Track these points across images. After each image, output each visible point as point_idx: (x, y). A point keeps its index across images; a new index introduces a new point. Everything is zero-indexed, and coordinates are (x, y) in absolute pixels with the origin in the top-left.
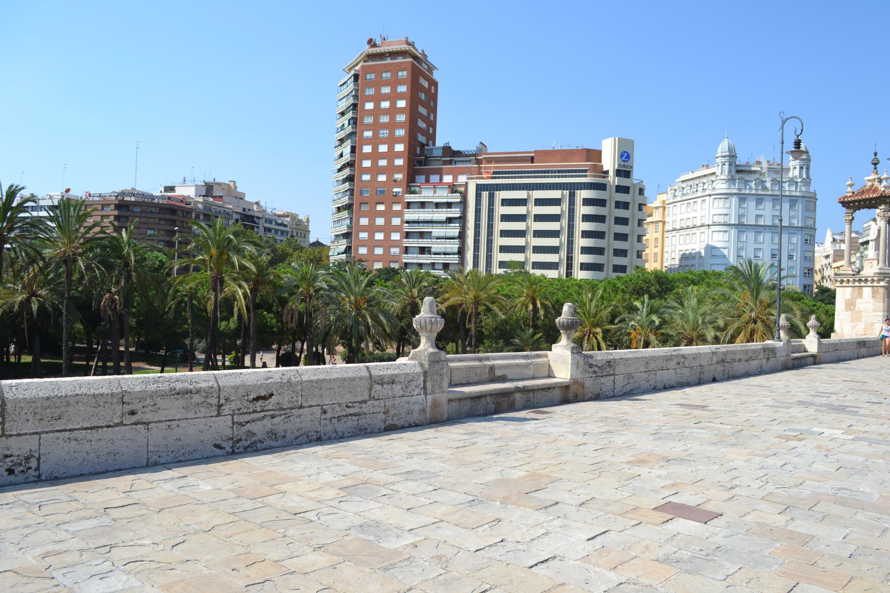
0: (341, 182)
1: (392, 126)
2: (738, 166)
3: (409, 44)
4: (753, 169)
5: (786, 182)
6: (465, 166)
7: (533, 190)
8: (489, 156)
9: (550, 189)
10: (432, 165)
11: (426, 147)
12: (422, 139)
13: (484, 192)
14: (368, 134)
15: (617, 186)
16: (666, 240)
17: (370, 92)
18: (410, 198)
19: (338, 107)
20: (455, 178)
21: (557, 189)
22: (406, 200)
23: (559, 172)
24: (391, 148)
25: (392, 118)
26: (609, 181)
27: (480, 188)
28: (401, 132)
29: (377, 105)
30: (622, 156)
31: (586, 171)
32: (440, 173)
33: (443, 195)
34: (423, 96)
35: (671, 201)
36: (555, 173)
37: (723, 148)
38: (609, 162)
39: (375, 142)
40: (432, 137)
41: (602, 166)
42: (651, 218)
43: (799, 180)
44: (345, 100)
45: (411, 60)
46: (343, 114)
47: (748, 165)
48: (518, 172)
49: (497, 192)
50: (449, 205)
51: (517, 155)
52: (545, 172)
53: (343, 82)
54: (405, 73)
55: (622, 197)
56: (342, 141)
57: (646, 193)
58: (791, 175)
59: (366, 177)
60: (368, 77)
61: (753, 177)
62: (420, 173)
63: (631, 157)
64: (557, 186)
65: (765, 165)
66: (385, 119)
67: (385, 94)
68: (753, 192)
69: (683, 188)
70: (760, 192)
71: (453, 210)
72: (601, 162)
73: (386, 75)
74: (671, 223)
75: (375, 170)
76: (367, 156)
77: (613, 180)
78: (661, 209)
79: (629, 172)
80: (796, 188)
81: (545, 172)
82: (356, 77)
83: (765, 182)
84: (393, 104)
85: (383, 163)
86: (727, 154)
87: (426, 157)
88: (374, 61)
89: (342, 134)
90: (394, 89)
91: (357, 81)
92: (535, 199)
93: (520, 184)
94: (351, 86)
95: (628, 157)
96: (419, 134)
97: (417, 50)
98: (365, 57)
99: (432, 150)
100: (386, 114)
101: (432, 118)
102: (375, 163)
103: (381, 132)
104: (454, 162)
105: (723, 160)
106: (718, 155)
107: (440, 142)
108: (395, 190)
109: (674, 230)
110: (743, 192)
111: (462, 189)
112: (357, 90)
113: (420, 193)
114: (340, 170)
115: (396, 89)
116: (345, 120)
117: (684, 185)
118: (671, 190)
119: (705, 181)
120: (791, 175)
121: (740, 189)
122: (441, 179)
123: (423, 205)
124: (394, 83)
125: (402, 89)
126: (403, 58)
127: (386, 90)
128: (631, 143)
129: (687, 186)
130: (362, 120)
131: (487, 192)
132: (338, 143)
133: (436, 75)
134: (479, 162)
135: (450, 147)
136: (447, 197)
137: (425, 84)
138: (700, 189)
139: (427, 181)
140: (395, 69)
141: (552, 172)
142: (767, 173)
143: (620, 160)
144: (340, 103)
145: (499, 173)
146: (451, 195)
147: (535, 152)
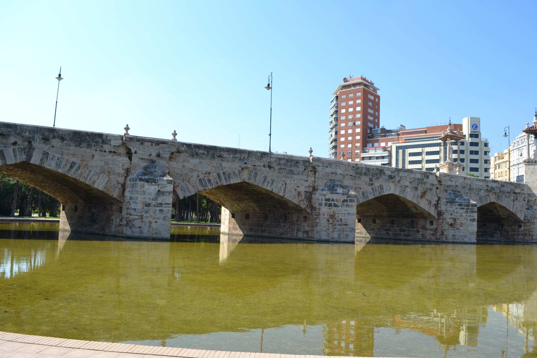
0: (331, 149)
3: (362, 78)
6: (391, 137)
7: (425, 147)
8: (407, 131)
9: (434, 146)
10: (376, 138)
11: (373, 129)
12: (371, 125)
13: (400, 150)
14: (343, 125)
15: (470, 143)
16: (511, 172)
17: (343, 104)
18: (363, 155)
20: (387, 144)
21: (437, 146)
22: (362, 156)
26: (466, 140)
27: (398, 148)
28: (358, 123)
29: (347, 110)
30: (473, 126)
33: (380, 153)
34: (371, 104)
35: (512, 149)
36: (437, 138)
38: (466, 131)
39: (346, 128)
40: (378, 124)
41: (463, 133)
42: (503, 159)
44: (332, 109)
45: (362, 87)
46: (332, 115)
48: (418, 139)
49: (407, 150)
50: (383, 157)
51: (418, 130)
52: (432, 138)
53: (332, 100)
54: (360, 94)
55: (474, 148)
56: (332, 129)
57: (490, 146)
59: (342, 146)
60: (343, 97)
62: (369, 142)
63: (478, 127)
64: (434, 145)
67: (351, 105)
69: (518, 142)
71: (384, 160)
72: (462, 131)
73: (351, 95)
74: (512, 161)
75: (346, 142)
76: (343, 136)
77: (468, 139)
78: (508, 154)
79: (478, 135)
81: (432, 138)
82: (337, 97)
84: (355, 109)
87: (372, 134)
88: (345, 89)
89: (332, 126)
90: (355, 102)
91: (338, 99)
92: (426, 152)
93: (415, 145)
94: (335, 102)
95: (476, 127)
96: (369, 123)
97: (368, 82)
98: (341, 87)
99: (378, 130)
100: (352, 114)
101: (377, 114)
102: (346, 139)
103: (349, 123)
107: (380, 127)
108: (356, 151)
109: (514, 165)
111: (389, 149)
112: (337, 104)
113: (369, 152)
114: (332, 143)
115: (356, 102)
116: (332, 119)
122: (380, 145)
123: (370, 158)
124: (355, 99)
125: (359, 101)
126: (360, 86)
127: (351, 103)
128: (479, 119)
129: (520, 140)
130: (340, 118)
131: (402, 150)
132: (330, 130)
133: (379, 93)
134: (398, 135)
135: (384, 129)
136: (381, 153)
137: (372, 98)
139: (373, 146)
140: (355, 92)
143: (472, 129)
144: (331, 110)
145: (407, 140)
146: (383, 152)
147: (427, 128)
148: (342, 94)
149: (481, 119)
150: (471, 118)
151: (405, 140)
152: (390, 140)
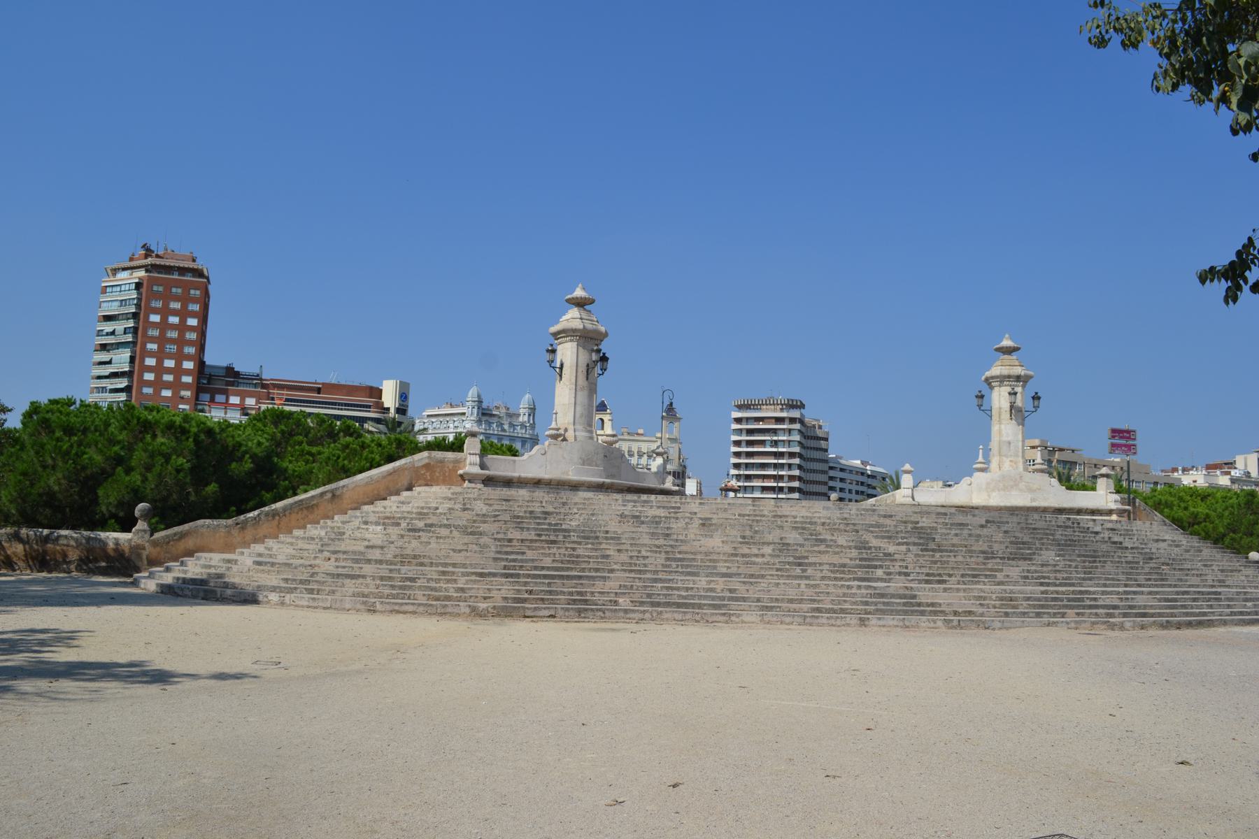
1: (181, 342)
2: (483, 409)
4: (494, 413)
5: (518, 426)
17: (158, 304)
19: (100, 307)
20: (243, 400)
23: (346, 405)
24: (179, 364)
25: (182, 335)
31: (370, 407)
32: (226, 393)
37: (472, 393)
38: (389, 399)
43: (528, 425)
47: (488, 409)
54: (198, 292)
58: (521, 419)
59: (148, 390)
60: (155, 288)
61: (495, 420)
65: (504, 411)
66: (173, 334)
68: (496, 432)
69: (433, 422)
70: (500, 433)
72: (381, 399)
75: (158, 384)
80: (526, 431)
83: (503, 424)
85: (168, 378)
86: (476, 399)
88: (159, 273)
95: (406, 398)
100: (176, 329)
103: (168, 347)
104: (236, 384)
105: (473, 404)
106: (468, 399)
110: (488, 432)
112: (139, 299)
117: (434, 420)
118: (420, 422)
119: (455, 419)
120: (521, 419)
121: (486, 430)
122: (227, 399)
124: (186, 300)
126: (194, 276)
127: (176, 305)
128: (409, 384)
135: (234, 368)
138: (451, 426)
139: (212, 400)
141: (339, 404)
142: (505, 417)
147: (323, 384)
148: (152, 282)
149: (411, 386)
150: (400, 382)
151: (287, 400)
152: (251, 395)
